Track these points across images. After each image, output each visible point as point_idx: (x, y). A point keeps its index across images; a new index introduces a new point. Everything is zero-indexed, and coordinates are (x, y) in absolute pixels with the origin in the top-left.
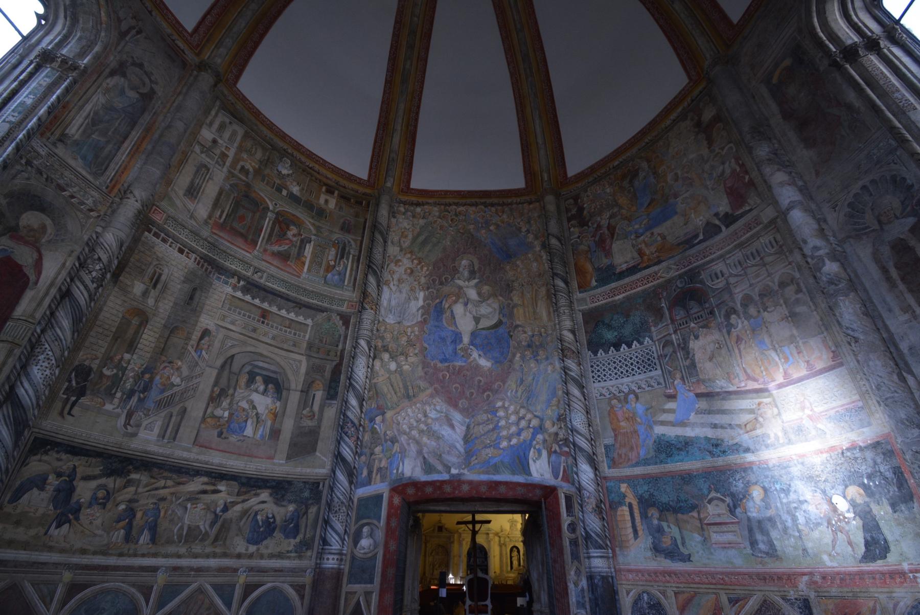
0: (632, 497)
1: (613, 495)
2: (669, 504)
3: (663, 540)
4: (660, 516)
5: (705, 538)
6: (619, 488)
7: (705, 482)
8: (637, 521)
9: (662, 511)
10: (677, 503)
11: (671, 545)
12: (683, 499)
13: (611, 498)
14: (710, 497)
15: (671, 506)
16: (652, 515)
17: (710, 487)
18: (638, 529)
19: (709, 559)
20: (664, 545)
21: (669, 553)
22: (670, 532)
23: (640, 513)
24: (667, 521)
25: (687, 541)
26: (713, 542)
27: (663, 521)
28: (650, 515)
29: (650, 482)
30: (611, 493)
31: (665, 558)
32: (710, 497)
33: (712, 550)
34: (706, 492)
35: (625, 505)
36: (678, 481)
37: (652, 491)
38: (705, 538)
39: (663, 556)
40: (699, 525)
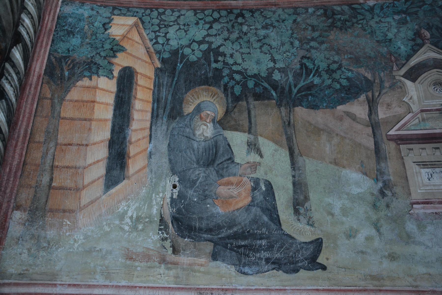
0: (141, 52)
1: (75, 41)
2: (269, 78)
3: (222, 190)
4: (227, 112)
5: (387, 185)
6: (106, 26)
7: (403, 22)
8: (135, 125)
9: (237, 99)
10: (298, 76)
11: (248, 208)
12: (323, 65)
13: (62, 47)
14: (413, 62)
15: (275, 85)
16: (198, 109)
17: (418, 34)
18: (132, 150)
19: (392, 257)
20: (220, 210)
21: (236, 236)
22: (254, 166)
23: (157, 100)
24: (250, 132)
25: (312, 195)
26: (415, 197)
27: (235, 128)
28: (189, 109)
29: (215, 20)
30: (70, 33)
31: (215, 257)
32: (413, 62)
33: (411, 227)
34: (403, 49)
35: (109, 74)
36: (314, 21)
37: (217, 41)
38: (387, 185)
39: (209, 247)
40: (370, 143)
